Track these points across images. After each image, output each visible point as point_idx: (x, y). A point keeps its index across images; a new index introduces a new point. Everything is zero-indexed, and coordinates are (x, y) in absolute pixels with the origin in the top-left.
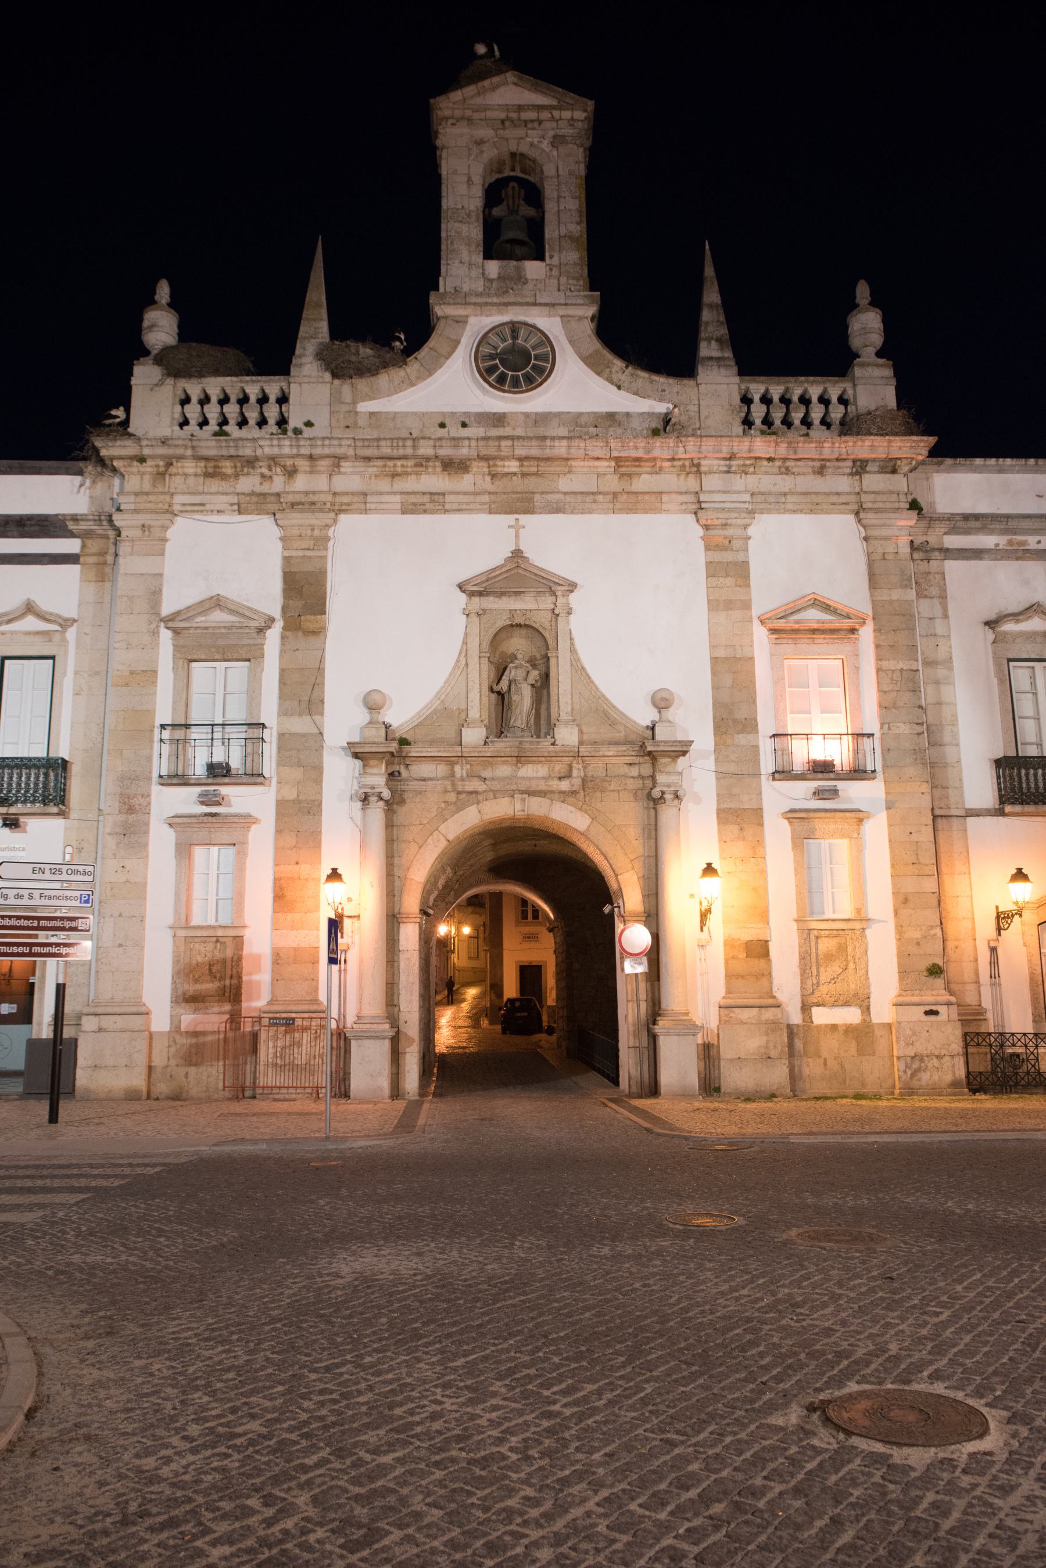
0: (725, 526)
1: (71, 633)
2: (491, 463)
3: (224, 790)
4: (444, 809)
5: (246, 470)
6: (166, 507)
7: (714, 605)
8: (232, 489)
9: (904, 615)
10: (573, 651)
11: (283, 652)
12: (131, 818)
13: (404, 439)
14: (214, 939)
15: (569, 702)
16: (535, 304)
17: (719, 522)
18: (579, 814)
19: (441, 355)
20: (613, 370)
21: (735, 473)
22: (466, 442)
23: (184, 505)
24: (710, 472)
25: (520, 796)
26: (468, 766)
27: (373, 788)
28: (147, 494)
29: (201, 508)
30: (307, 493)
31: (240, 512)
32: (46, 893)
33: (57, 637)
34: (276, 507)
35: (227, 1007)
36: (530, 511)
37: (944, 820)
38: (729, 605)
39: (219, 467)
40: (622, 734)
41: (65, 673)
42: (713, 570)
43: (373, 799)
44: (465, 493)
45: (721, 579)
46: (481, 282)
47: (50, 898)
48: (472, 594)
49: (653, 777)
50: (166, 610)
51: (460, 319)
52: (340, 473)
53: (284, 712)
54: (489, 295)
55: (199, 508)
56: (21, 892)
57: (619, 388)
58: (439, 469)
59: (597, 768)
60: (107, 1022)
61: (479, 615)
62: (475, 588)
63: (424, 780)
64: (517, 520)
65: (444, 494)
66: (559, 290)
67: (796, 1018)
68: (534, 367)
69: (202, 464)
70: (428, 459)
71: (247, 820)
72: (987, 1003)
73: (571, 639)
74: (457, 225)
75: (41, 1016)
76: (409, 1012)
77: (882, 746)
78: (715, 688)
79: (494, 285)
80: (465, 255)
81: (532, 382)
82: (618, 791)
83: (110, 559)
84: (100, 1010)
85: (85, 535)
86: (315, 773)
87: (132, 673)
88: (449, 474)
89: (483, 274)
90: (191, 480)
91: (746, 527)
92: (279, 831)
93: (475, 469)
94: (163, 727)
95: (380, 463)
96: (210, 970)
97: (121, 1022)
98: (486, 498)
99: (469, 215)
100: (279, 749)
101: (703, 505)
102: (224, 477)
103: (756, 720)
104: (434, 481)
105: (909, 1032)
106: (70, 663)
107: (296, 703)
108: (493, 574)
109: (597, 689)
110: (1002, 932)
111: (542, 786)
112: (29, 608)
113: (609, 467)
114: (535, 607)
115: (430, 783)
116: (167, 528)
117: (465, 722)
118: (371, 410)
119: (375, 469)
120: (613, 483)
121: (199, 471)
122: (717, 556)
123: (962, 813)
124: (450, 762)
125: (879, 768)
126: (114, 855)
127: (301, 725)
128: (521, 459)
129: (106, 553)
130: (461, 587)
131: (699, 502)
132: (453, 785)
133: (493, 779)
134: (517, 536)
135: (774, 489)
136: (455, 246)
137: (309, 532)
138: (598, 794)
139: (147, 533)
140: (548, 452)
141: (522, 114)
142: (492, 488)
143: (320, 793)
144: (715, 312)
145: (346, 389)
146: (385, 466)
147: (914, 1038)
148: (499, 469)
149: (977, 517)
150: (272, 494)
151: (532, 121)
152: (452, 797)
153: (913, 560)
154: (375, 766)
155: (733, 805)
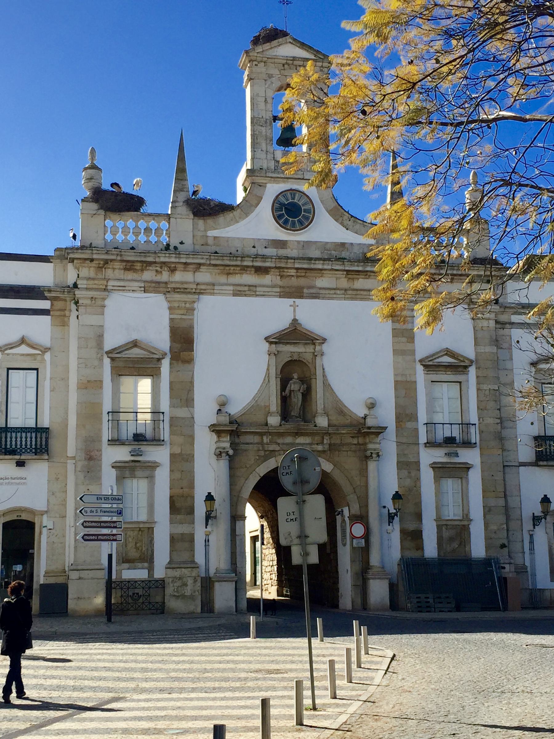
1: (47, 356)
2: (281, 270)
3: (143, 448)
5: (148, 268)
6: (104, 287)
7: (396, 352)
8: (140, 278)
10: (324, 376)
11: (171, 372)
12: (92, 463)
13: (237, 257)
14: (138, 529)
15: (322, 403)
16: (303, 179)
18: (327, 463)
19: (252, 205)
20: (344, 219)
22: (270, 260)
23: (113, 286)
26: (270, 437)
27: (224, 448)
28: (93, 279)
30: (182, 283)
31: (145, 292)
32: (104, 510)
33: (39, 358)
34: (165, 290)
35: (146, 565)
36: (301, 297)
39: (133, 266)
40: (349, 420)
41: (45, 378)
42: (396, 333)
43: (224, 455)
44: (267, 287)
47: (105, 512)
48: (271, 343)
49: (365, 444)
50: (107, 347)
51: (261, 184)
52: (199, 272)
53: (172, 406)
55: (123, 289)
56: (93, 509)
57: (347, 229)
58: (253, 272)
59: (336, 440)
60: (84, 574)
61: (275, 355)
62: (274, 340)
63: (248, 444)
64: (294, 302)
65: (256, 286)
69: (124, 264)
70: (248, 267)
72: (527, 564)
73: (323, 369)
74: (260, 128)
75: (39, 571)
77: (479, 430)
78: (396, 397)
82: (347, 451)
83: (67, 313)
84: (79, 568)
85: (53, 299)
86: (191, 438)
87: (89, 381)
88: (258, 275)
89: (274, 157)
90: (117, 271)
92: (171, 471)
93: (272, 273)
95: (222, 268)
97: (91, 574)
98: (278, 290)
99: (266, 122)
100: (171, 426)
102: (135, 271)
104: (249, 279)
106: (47, 372)
107: (179, 400)
108: (283, 333)
109: (337, 397)
110: (536, 527)
113: (343, 274)
115: (251, 446)
116: (105, 299)
117: (269, 413)
118: (215, 235)
119: (219, 271)
120: (344, 283)
121: (122, 267)
122: (397, 326)
123: (517, 464)
124: (261, 434)
125: (478, 442)
126: (83, 483)
127: (182, 413)
128: (297, 269)
129: (65, 310)
130: (266, 339)
132: (263, 447)
133: (283, 444)
137: (183, 305)
138: (337, 452)
139: (93, 302)
140: (312, 266)
141: (295, 62)
145: (201, 223)
146: (224, 269)
148: (285, 273)
150: (163, 283)
151: (300, 66)
152: (262, 453)
154: (225, 437)
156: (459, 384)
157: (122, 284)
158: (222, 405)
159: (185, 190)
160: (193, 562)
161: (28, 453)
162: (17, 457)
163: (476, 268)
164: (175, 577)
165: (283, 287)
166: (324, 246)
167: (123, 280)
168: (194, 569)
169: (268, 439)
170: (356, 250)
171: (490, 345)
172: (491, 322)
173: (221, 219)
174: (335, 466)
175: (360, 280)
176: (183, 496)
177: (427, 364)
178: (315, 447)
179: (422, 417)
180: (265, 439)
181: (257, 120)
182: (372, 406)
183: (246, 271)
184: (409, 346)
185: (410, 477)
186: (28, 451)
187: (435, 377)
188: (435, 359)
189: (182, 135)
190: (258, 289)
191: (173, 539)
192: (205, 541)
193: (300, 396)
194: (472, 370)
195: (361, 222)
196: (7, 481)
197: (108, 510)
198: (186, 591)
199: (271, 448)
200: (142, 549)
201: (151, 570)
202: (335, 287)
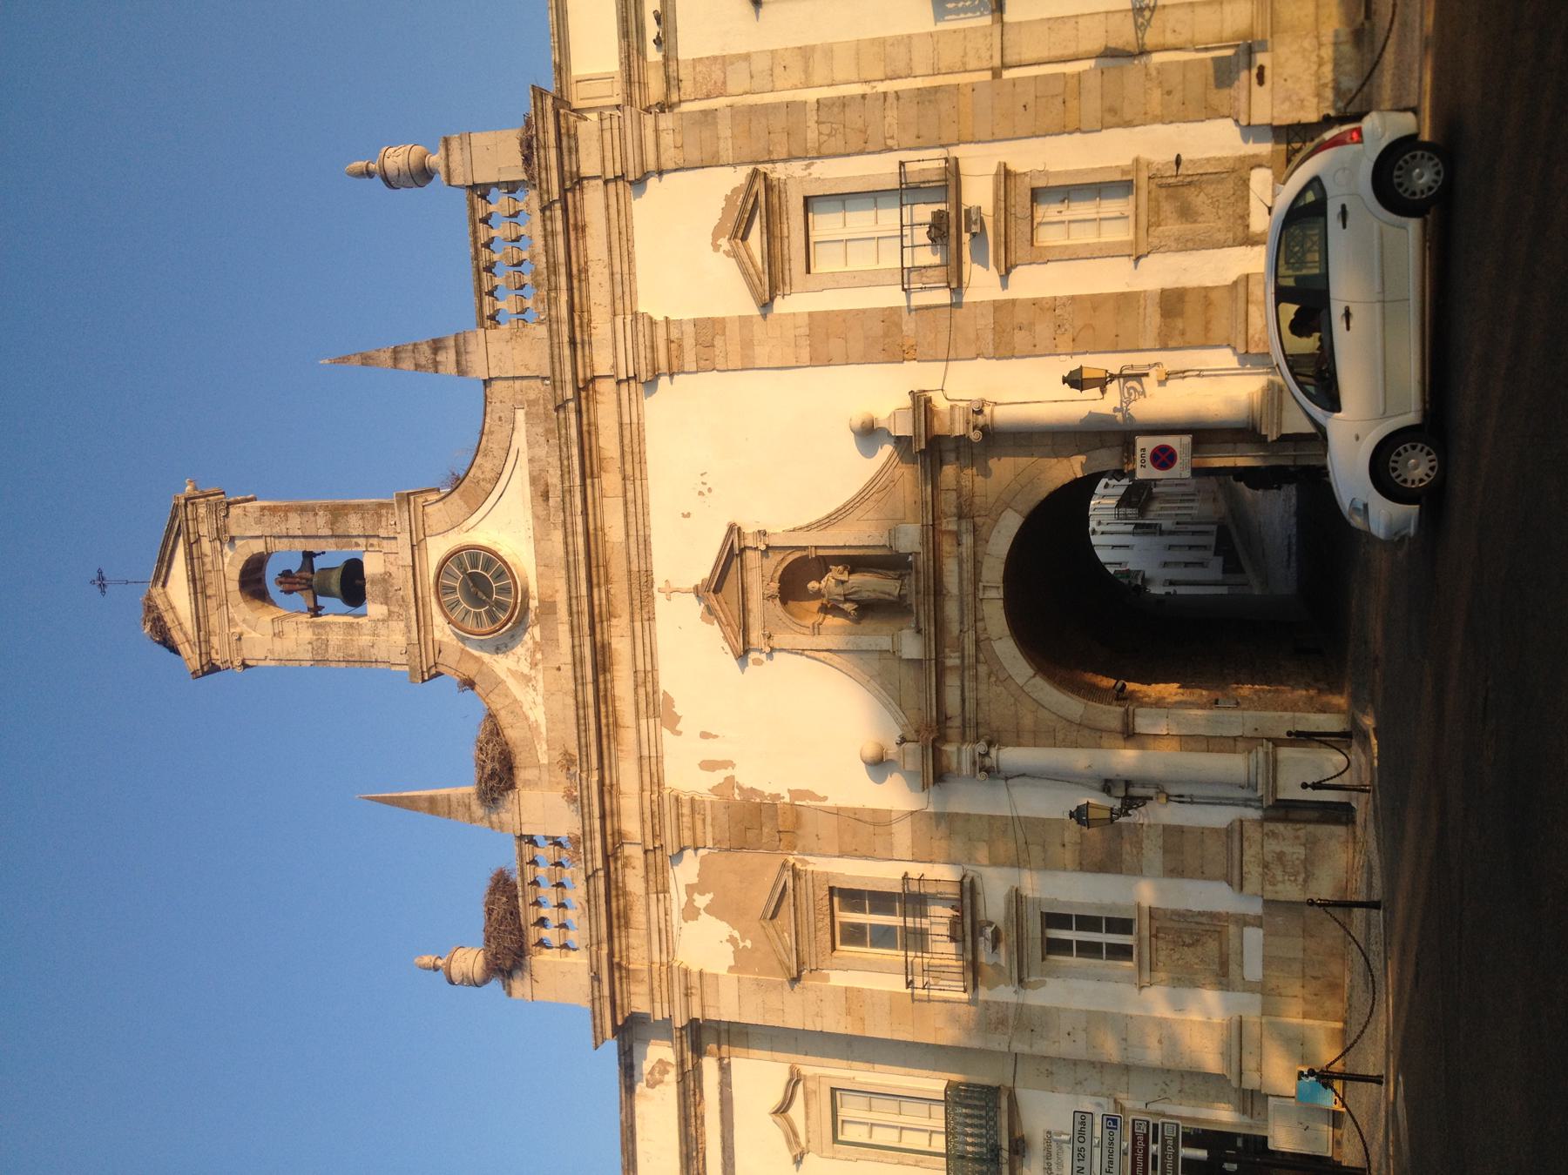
0: (653, 348)
1: (806, 1070)
4: (997, 678)
9: (750, 120)
10: (809, 527)
16: (414, 567)
17: (649, 356)
18: (1002, 523)
21: (590, 336)
22: (577, 649)
24: (592, 366)
25: (981, 592)
26: (947, 650)
27: (974, 763)
28: (652, 990)
29: (664, 932)
30: (643, 821)
31: (666, 891)
32: (1105, 1165)
35: (1232, 929)
36: (648, 573)
37: (1007, 52)
38: (747, 344)
43: (987, 762)
45: (717, 352)
46: (393, 624)
47: (1111, 1162)
51: (437, 652)
54: (408, 619)
55: (665, 937)
63: (963, 701)
66: (395, 538)
68: (486, 569)
71: (1017, 899)
74: (330, 650)
76: (1244, 725)
79: (392, 608)
81: (503, 572)
87: (848, 1013)
89: (384, 621)
91: (652, 323)
94: (909, 984)
96: (1189, 946)
98: (638, 625)
101: (631, 374)
102: (627, 908)
103: (884, 310)
105: (1286, 106)
108: (723, 619)
111: (968, 566)
114: (758, 570)
115: (967, 694)
117: (894, 653)
120: (610, 481)
126: (1055, 1042)
131: (628, 379)
133: (962, 623)
134: (677, 591)
136: (355, 652)
142: (626, 618)
143: (980, 817)
144: (403, 355)
145: (522, 775)
147: (1294, 98)
149: (624, 21)
153: (680, 101)
154: (949, 758)
156: (811, 200)
158: (879, 765)
159: (467, 801)
160: (1228, 831)
161: (995, 1123)
162: (1005, 1154)
163: (543, 175)
164: (1263, 875)
165: (632, 614)
166: (541, 523)
167: (649, 934)
168: (1245, 835)
169: (952, 655)
170: (541, 452)
171: (715, 124)
172: (662, 125)
173: (512, 734)
174: (1008, 506)
175: (601, 443)
176: (1081, 844)
177: (767, 288)
178: (966, 549)
179: (892, 297)
180: (952, 660)
181: (318, 654)
182: (869, 434)
183: (606, 690)
184: (733, 331)
185: (1032, 324)
186: (992, 1132)
187: (798, 264)
188: (754, 266)
190: (640, 666)
191: (1175, 870)
192: (1180, 802)
193: (856, 579)
194: (779, 172)
195: (484, 438)
196: (1054, 1167)
197: (1106, 1153)
198: (1295, 856)
199: (970, 649)
200: (1198, 934)
201: (1243, 921)
202: (621, 500)
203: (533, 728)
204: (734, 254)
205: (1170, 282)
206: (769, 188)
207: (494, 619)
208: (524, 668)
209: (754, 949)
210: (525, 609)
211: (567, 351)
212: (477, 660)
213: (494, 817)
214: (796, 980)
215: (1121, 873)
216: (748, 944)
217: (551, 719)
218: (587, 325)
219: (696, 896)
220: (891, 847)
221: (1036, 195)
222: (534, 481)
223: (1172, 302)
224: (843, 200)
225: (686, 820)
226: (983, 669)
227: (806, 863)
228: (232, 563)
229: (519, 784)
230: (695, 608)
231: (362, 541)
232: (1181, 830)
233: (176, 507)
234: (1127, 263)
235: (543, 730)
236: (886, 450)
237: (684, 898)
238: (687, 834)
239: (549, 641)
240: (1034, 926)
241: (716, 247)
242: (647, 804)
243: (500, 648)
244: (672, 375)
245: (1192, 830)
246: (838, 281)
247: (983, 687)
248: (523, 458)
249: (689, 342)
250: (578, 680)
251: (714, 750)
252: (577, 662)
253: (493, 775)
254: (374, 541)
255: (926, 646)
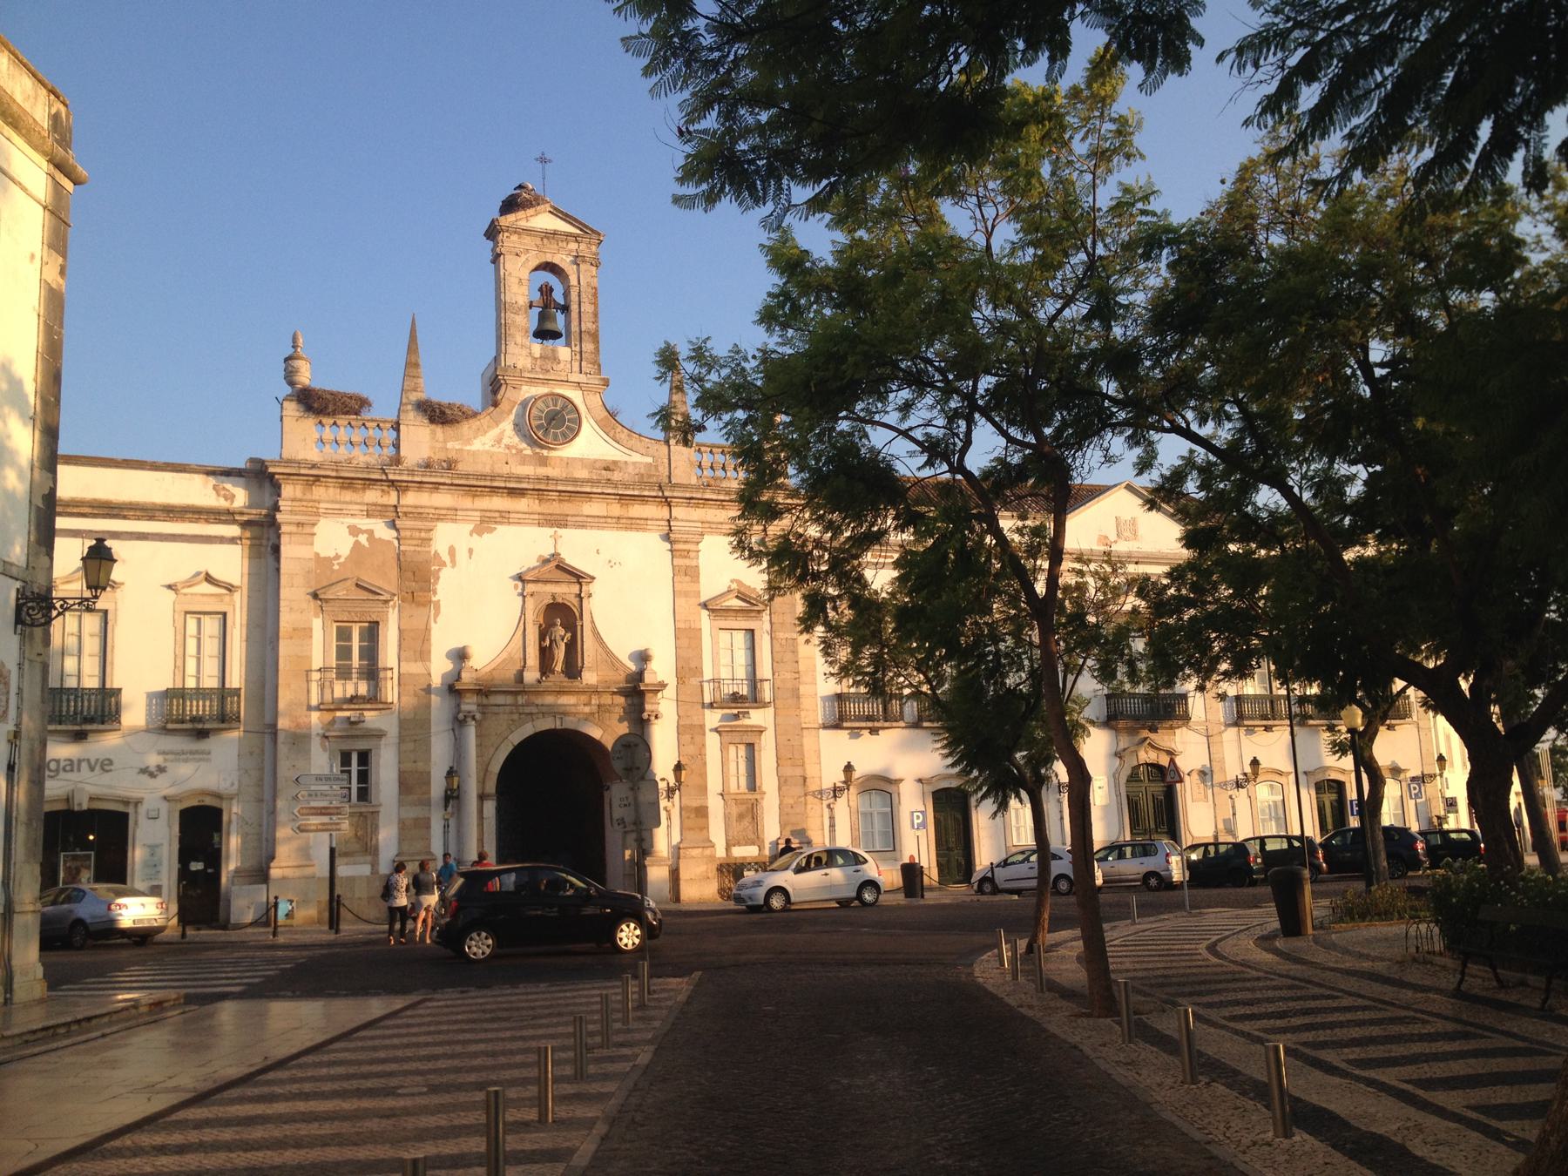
1: (237, 596)
10: (593, 622)
28: (300, 500)
30: (416, 507)
31: (368, 516)
35: (369, 858)
36: (566, 526)
38: (686, 594)
43: (469, 719)
55: (339, 513)
67: (720, 852)
80: (519, 339)
87: (294, 630)
90: (331, 490)
98: (536, 517)
102: (355, 490)
104: (499, 503)
112: (209, 579)
120: (616, 509)
135: (715, 520)
140: (579, 489)
145: (439, 429)
152: (516, 717)
155: (688, 722)
157: (337, 506)
160: (432, 854)
166: (592, 464)
167: (337, 502)
170: (630, 469)
179: (708, 674)
180: (521, 700)
189: (413, 320)
190: (512, 515)
191: (403, 826)
194: (765, 616)
199: (527, 710)
201: (374, 865)
203: (469, 441)
204: (729, 591)
205: (711, 810)
206: (759, 612)
207: (539, 427)
208: (506, 441)
209: (333, 571)
210: (542, 447)
211: (688, 495)
212: (511, 411)
213: (409, 407)
214: (315, 596)
215: (400, 794)
216: (336, 567)
217: (474, 454)
218: (697, 506)
219: (366, 536)
220: (408, 660)
221: (750, 747)
222: (615, 462)
223: (702, 812)
224: (752, 648)
225: (417, 534)
226: (516, 717)
227: (394, 607)
228: (563, 260)
229: (433, 427)
230: (547, 551)
231: (578, 349)
232: (428, 827)
233: (599, 234)
234: (720, 791)
235: (468, 448)
236: (633, 667)
237: (364, 528)
238: (408, 534)
239: (524, 460)
240: (362, 745)
241: (732, 581)
242: (427, 511)
243: (518, 427)
244: (671, 551)
245: (429, 833)
246: (715, 642)
247: (506, 717)
248: (626, 458)
249: (687, 562)
250: (509, 478)
251: (462, 555)
252: (519, 479)
253: (443, 413)
254: (578, 357)
255: (532, 686)
